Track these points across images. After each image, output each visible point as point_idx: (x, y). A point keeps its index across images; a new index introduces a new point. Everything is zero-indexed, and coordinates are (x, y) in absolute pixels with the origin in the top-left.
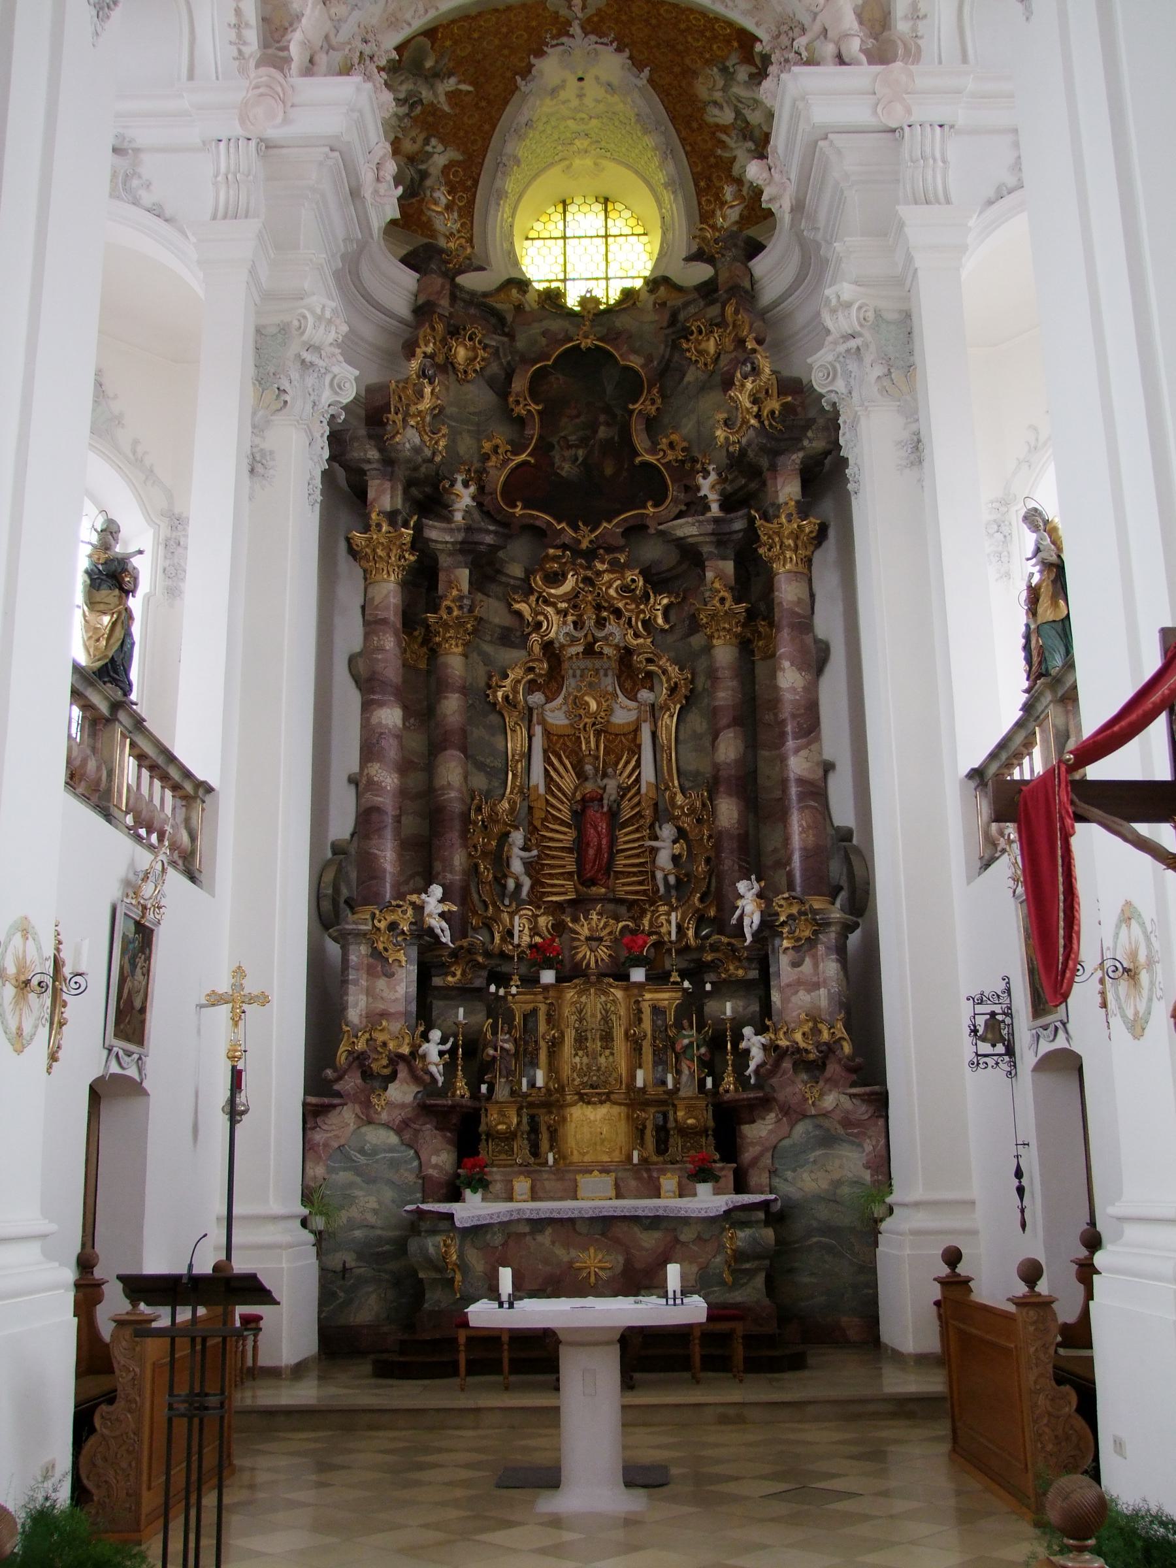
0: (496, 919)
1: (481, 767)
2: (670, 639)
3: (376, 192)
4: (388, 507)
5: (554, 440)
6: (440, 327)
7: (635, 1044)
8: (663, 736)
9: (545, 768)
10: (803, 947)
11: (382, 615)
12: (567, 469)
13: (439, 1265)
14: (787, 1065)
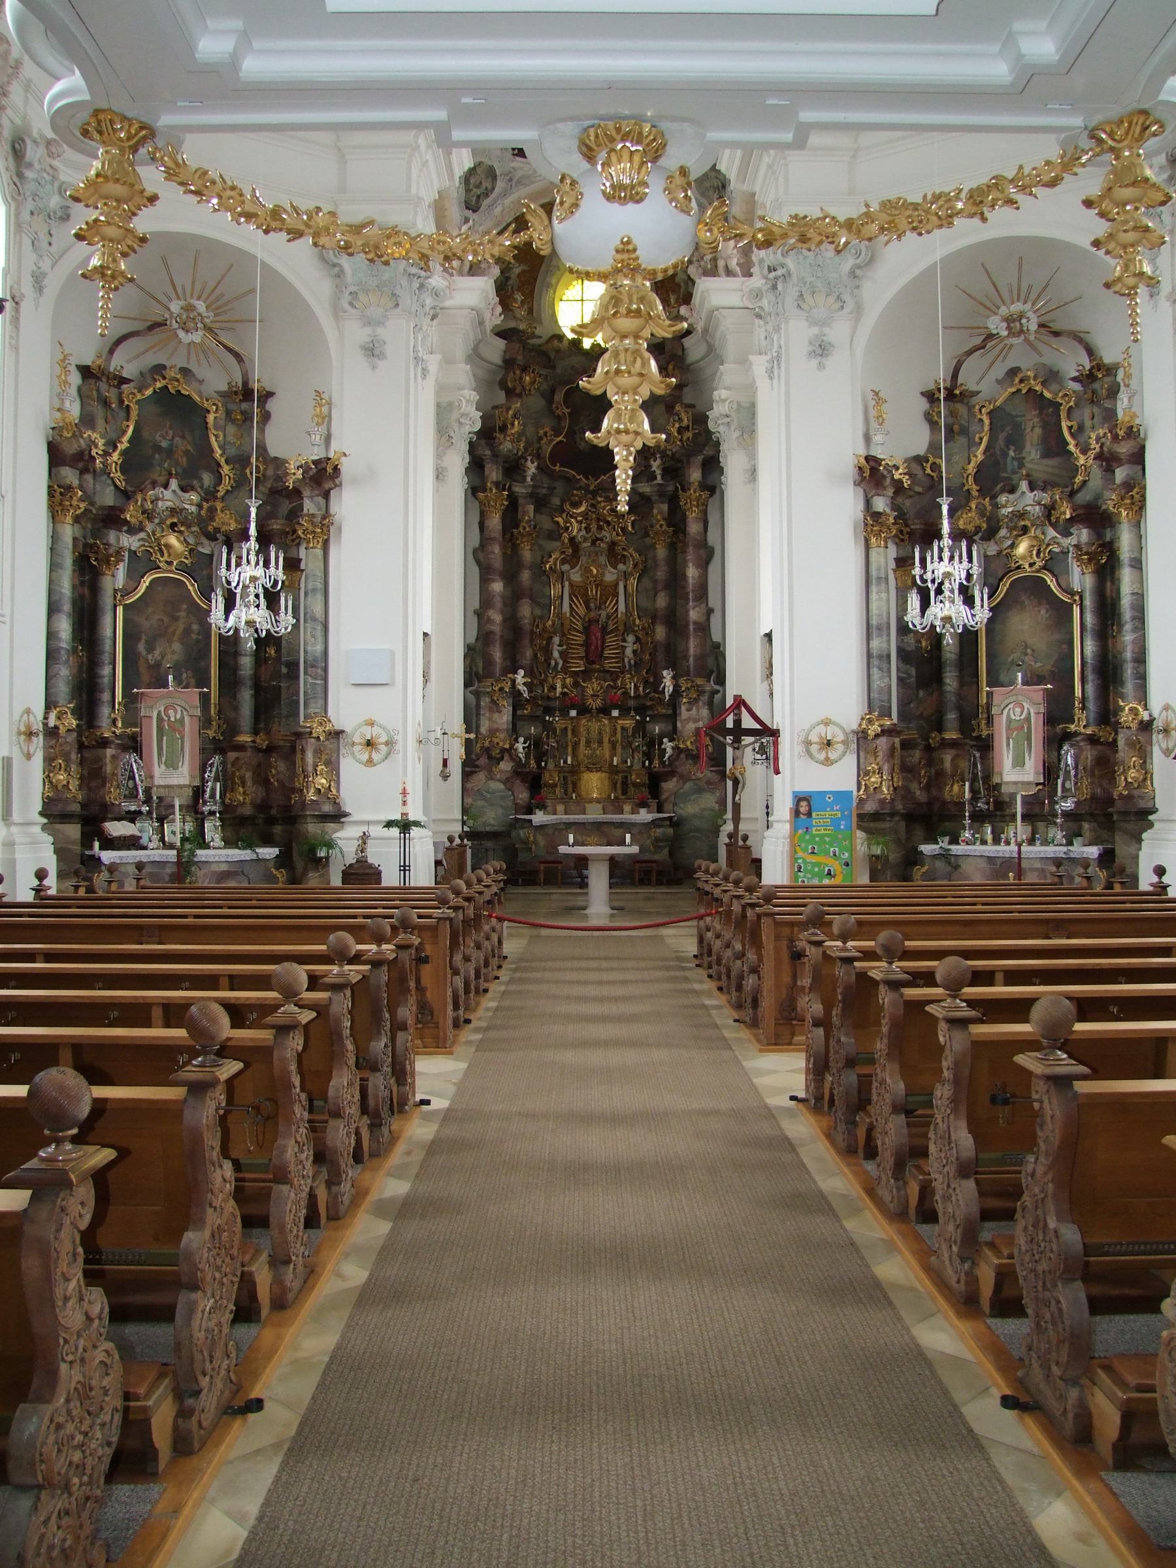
0: (545, 680)
1: (538, 604)
4: (495, 479)
5: (576, 428)
6: (518, 372)
7: (613, 745)
8: (630, 589)
10: (693, 702)
11: (493, 535)
13: (525, 842)
14: (683, 756)
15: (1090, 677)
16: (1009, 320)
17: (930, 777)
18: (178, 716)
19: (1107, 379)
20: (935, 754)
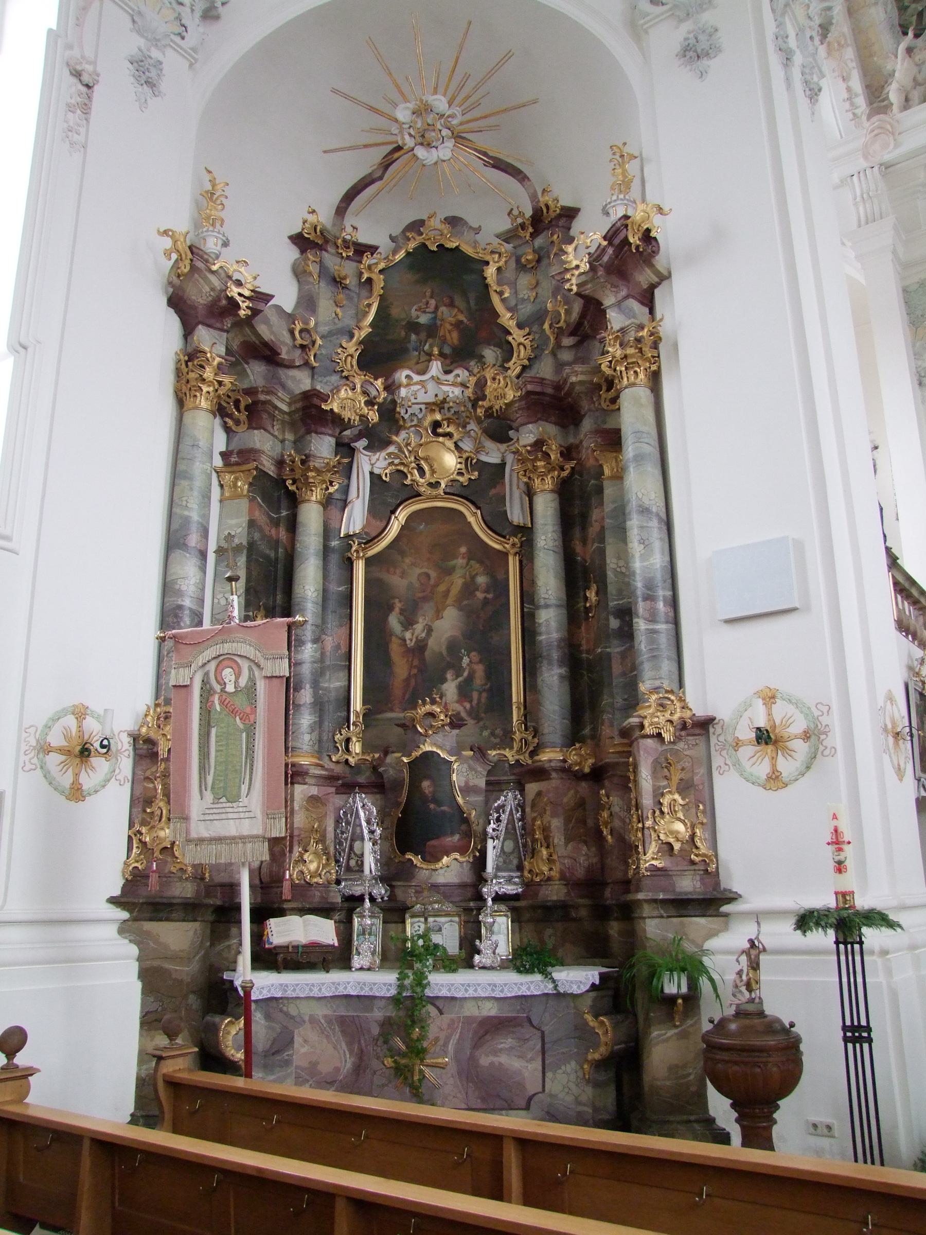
18: (243, 681)
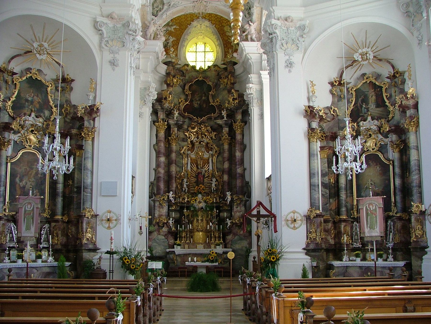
1: (178, 166)
2: (216, 141)
3: (161, 57)
5: (194, 99)
6: (171, 77)
8: (214, 161)
9: (191, 166)
12: (196, 106)
13: (172, 260)
14: (234, 226)
15: (398, 193)
16: (362, 55)
17: (335, 234)
19: (400, 77)
20: (337, 225)
